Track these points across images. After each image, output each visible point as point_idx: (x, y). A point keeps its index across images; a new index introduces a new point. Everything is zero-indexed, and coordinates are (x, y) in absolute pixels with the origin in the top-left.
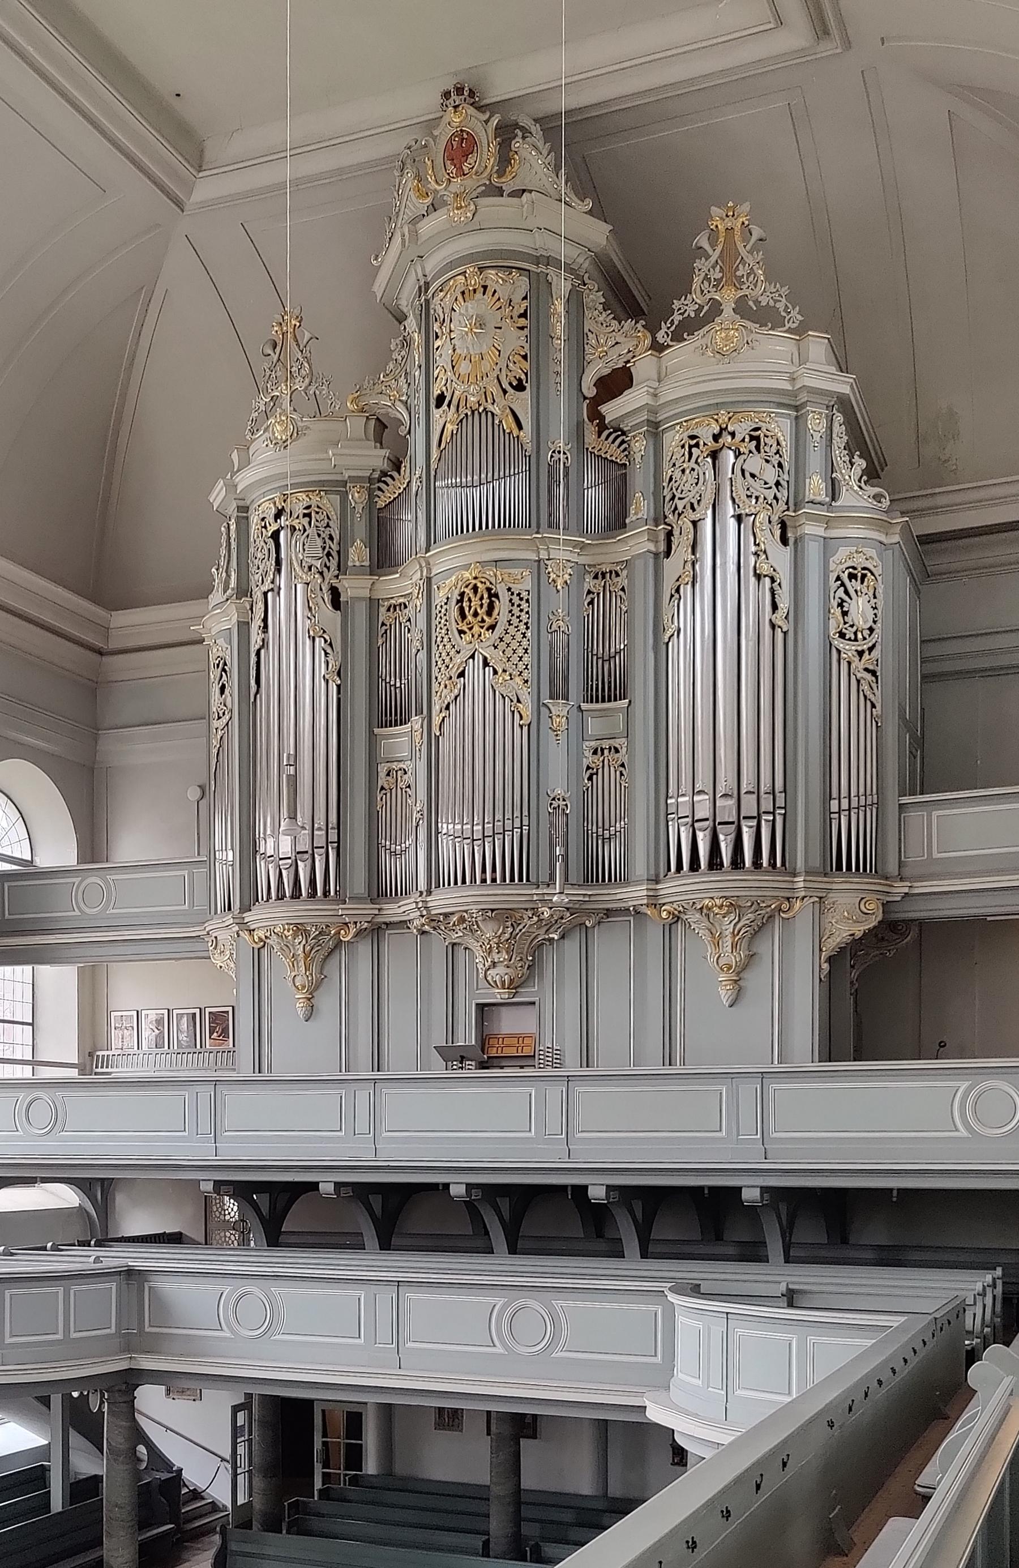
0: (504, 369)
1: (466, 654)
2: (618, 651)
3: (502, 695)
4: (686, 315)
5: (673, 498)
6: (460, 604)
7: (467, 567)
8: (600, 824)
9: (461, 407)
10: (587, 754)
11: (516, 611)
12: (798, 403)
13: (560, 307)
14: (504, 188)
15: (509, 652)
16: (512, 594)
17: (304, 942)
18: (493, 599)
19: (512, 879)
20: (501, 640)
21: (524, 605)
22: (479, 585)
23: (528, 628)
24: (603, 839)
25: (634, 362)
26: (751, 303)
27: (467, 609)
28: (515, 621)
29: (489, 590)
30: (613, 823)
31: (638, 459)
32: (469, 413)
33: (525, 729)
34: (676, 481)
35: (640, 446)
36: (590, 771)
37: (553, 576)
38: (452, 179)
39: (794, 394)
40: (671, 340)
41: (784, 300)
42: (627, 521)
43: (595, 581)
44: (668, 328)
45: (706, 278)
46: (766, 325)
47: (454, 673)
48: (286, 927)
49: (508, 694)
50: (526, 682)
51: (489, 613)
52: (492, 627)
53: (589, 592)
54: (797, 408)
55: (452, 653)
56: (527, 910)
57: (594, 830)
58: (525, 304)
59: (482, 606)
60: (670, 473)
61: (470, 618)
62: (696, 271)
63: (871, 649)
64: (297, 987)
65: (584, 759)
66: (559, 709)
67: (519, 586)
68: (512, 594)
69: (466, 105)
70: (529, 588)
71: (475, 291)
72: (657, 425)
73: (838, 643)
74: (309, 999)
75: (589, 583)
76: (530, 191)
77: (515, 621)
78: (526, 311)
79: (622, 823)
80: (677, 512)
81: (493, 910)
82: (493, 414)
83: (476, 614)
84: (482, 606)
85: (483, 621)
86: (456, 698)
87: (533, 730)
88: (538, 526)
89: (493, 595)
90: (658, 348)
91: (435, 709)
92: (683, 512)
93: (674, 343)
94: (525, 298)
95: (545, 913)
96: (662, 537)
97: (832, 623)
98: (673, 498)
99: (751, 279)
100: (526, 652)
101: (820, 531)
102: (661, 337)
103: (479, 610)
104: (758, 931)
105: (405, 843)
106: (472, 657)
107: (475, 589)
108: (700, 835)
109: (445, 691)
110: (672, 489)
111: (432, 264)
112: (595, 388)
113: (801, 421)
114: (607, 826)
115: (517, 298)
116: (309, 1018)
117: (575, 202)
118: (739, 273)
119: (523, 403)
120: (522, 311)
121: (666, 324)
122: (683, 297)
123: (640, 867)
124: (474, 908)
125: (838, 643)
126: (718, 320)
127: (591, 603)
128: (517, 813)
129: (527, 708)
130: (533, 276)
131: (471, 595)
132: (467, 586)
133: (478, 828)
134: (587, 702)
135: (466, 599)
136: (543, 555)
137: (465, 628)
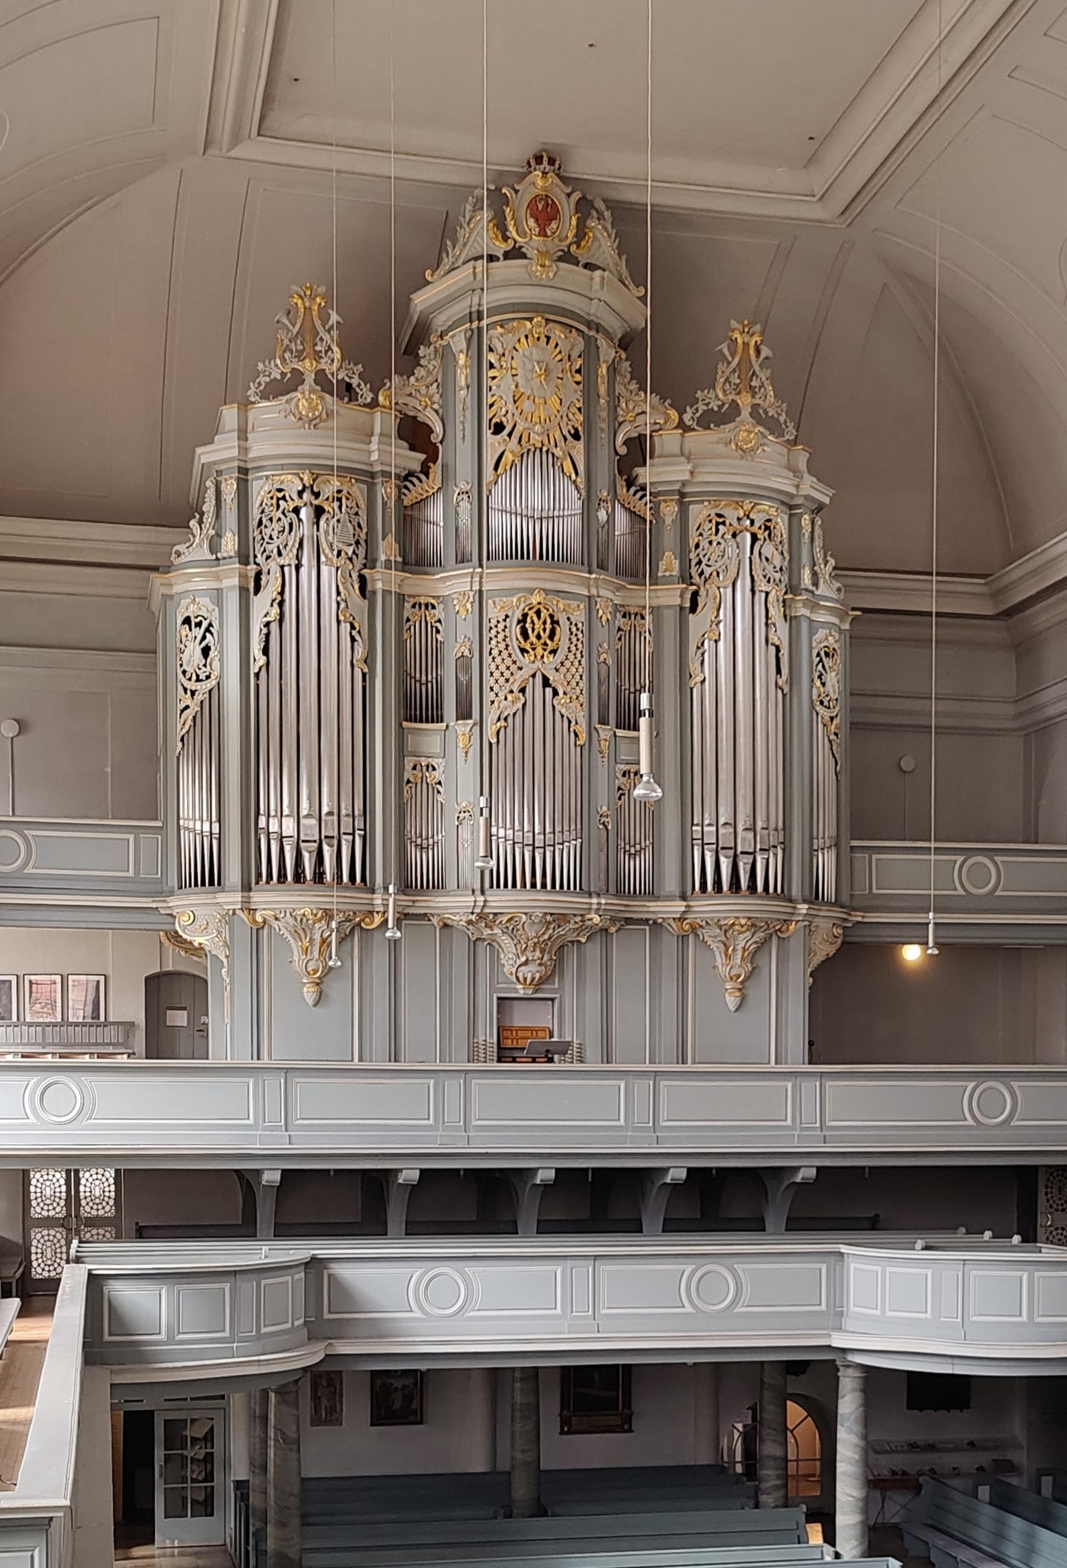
0: (565, 418)
1: (526, 672)
2: (643, 685)
3: (562, 716)
4: (710, 406)
5: (700, 563)
6: (522, 624)
7: (531, 591)
8: (627, 841)
9: (523, 442)
10: (618, 774)
11: (574, 639)
12: (793, 503)
13: (603, 370)
14: (579, 259)
15: (569, 677)
16: (571, 623)
17: (325, 927)
18: (555, 625)
19: (569, 887)
20: (562, 664)
21: (580, 636)
22: (543, 609)
23: (582, 656)
24: (630, 855)
25: (661, 435)
26: (761, 411)
27: (530, 631)
28: (573, 649)
29: (551, 616)
30: (638, 841)
31: (668, 520)
32: (533, 449)
33: (579, 749)
34: (703, 550)
35: (670, 511)
36: (620, 792)
37: (601, 612)
38: (534, 237)
39: (792, 496)
40: (697, 425)
41: (784, 414)
42: (660, 574)
43: (624, 619)
44: (694, 414)
45: (727, 380)
46: (774, 434)
47: (515, 689)
48: (314, 912)
49: (569, 716)
50: (582, 705)
51: (552, 637)
52: (554, 652)
53: (619, 629)
54: (791, 507)
55: (513, 668)
56: (575, 915)
57: (623, 846)
58: (580, 362)
59: (544, 630)
60: (696, 540)
61: (533, 638)
62: (720, 372)
63: (837, 715)
64: (308, 973)
65: (617, 781)
66: (605, 732)
67: (577, 618)
68: (571, 623)
69: (552, 174)
70: (583, 620)
71: (538, 339)
72: (682, 495)
73: (819, 708)
74: (318, 984)
75: (620, 621)
76: (604, 270)
77: (573, 649)
78: (580, 367)
79: (647, 842)
80: (703, 576)
81: (551, 914)
82: (553, 454)
83: (539, 637)
84: (544, 630)
85: (545, 644)
86: (514, 714)
87: (587, 750)
88: (590, 566)
89: (555, 622)
90: (686, 429)
91: (490, 716)
92: (709, 577)
93: (699, 429)
94: (580, 356)
95: (595, 920)
96: (688, 596)
97: (815, 691)
98: (700, 563)
99: (763, 390)
100: (581, 679)
101: (806, 612)
102: (687, 417)
103: (542, 633)
104: (765, 943)
105: (433, 837)
106: (534, 676)
107: (538, 613)
108: (722, 859)
109: (505, 702)
110: (698, 555)
111: (488, 300)
112: (624, 447)
113: (795, 519)
114: (632, 843)
115: (575, 354)
116: (318, 1002)
117: (632, 286)
118: (753, 384)
119: (579, 449)
120: (578, 367)
121: (691, 407)
122: (706, 391)
123: (671, 883)
124: (539, 913)
125: (819, 708)
126: (738, 419)
127: (620, 639)
128: (573, 827)
129: (582, 729)
130: (586, 337)
131: (535, 619)
132: (530, 609)
133: (539, 838)
134: (624, 729)
135: (529, 620)
136: (594, 592)
137: (528, 647)
